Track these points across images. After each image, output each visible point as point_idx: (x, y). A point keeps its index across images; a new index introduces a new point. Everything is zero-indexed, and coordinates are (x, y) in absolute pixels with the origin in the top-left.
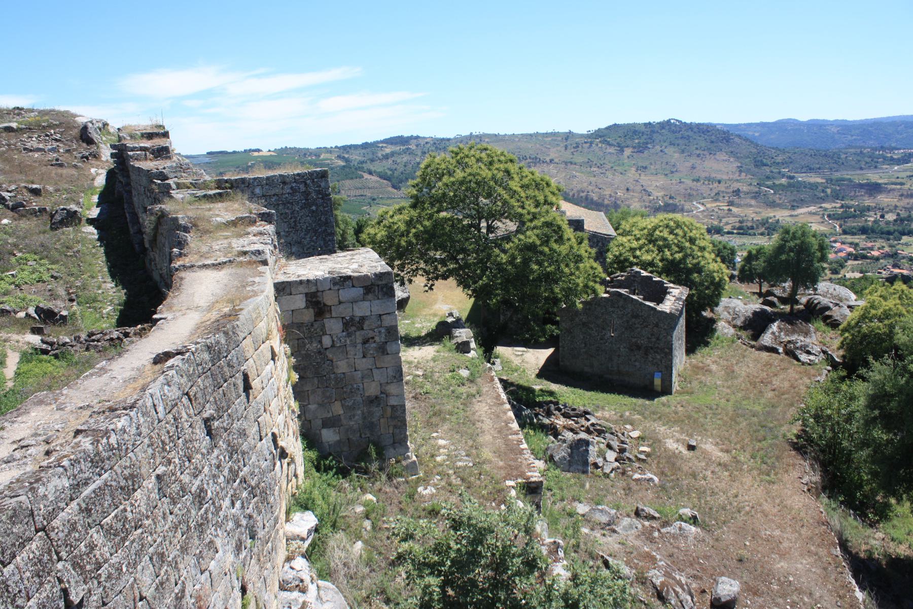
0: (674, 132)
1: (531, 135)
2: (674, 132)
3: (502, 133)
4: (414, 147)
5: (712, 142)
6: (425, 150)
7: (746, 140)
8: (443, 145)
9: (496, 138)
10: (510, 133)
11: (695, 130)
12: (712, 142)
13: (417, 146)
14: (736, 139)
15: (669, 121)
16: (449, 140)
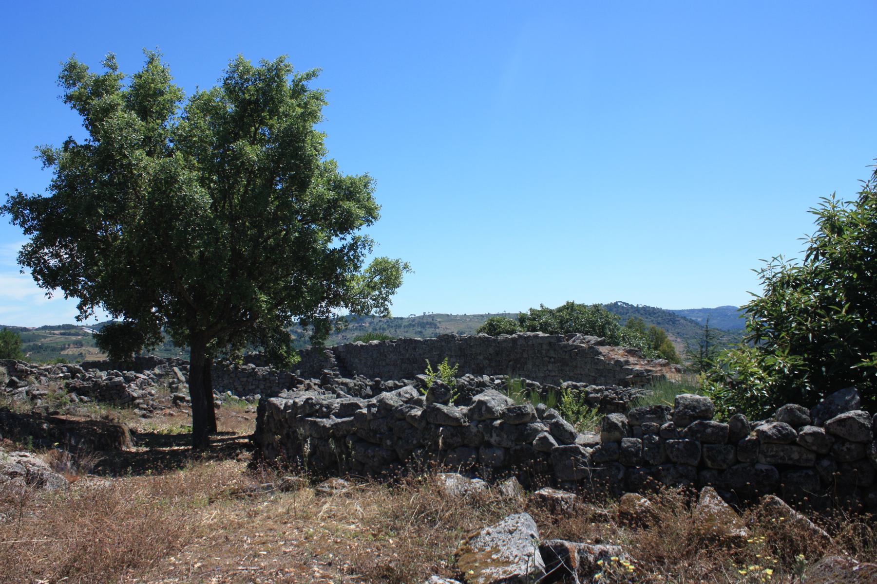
0: (621, 314)
1: (482, 316)
2: (621, 314)
3: (454, 314)
4: (368, 325)
5: (659, 323)
6: (378, 327)
7: (691, 321)
8: (395, 323)
9: (448, 318)
10: (461, 313)
11: (642, 312)
12: (659, 323)
13: (370, 323)
14: (682, 321)
15: (616, 303)
16: (402, 319)
